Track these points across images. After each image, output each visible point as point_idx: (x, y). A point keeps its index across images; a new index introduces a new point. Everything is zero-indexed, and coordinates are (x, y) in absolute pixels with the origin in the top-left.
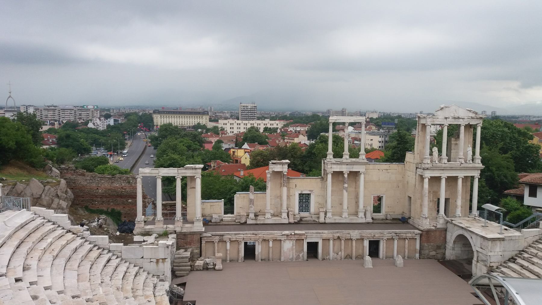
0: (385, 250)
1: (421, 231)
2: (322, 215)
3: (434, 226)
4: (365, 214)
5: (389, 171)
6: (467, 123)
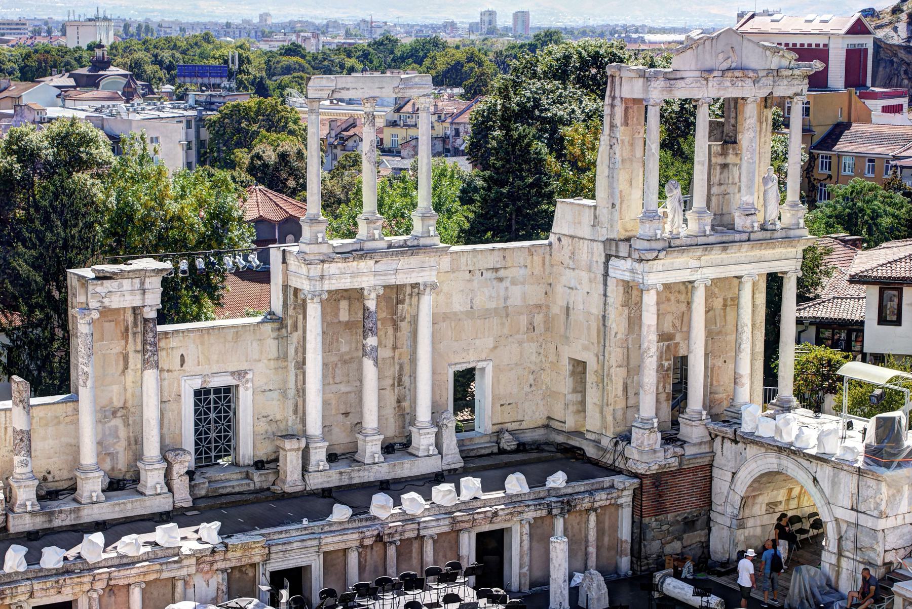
0: (526, 559)
1: (636, 475)
2: (291, 464)
4: (438, 445)
5: (502, 273)
6: (764, 93)
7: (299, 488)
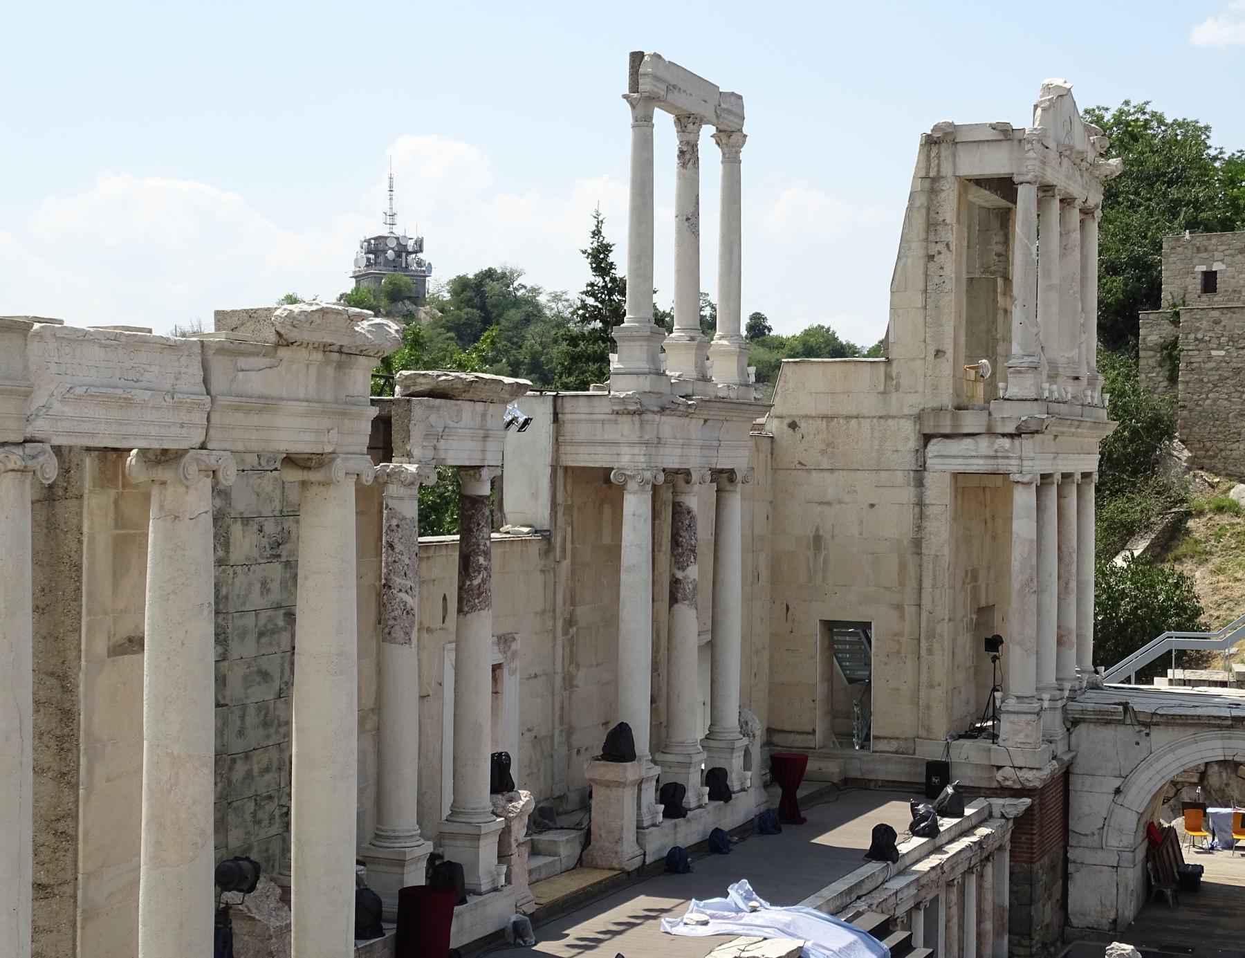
7: (637, 863)
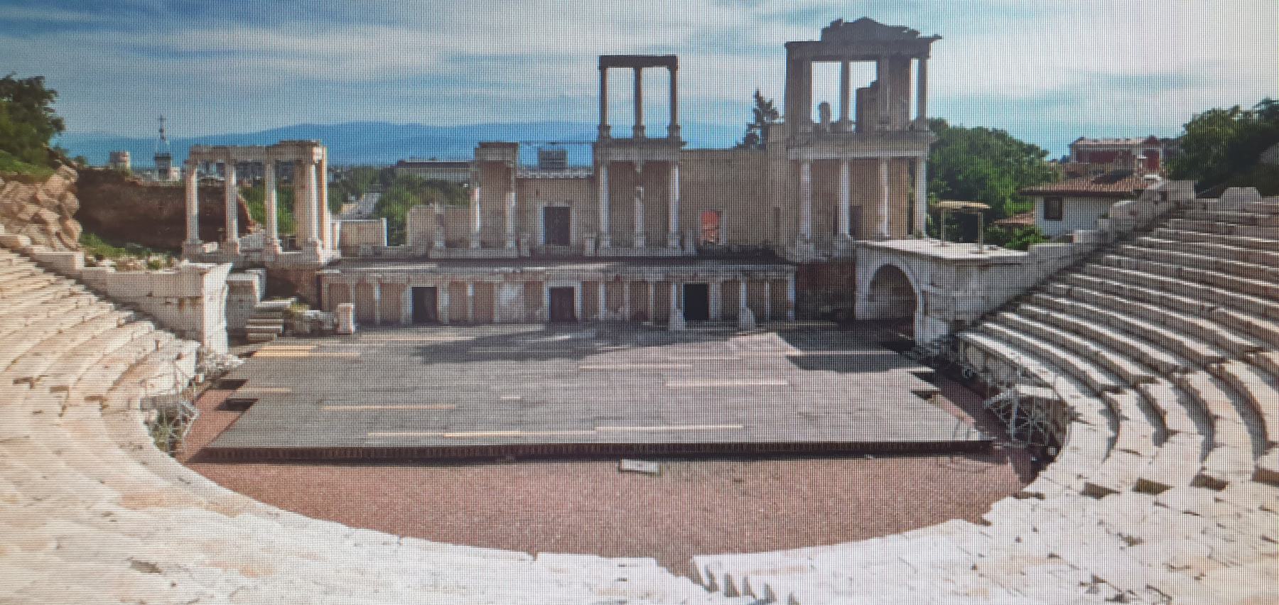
1: (798, 264)
3: (824, 255)
